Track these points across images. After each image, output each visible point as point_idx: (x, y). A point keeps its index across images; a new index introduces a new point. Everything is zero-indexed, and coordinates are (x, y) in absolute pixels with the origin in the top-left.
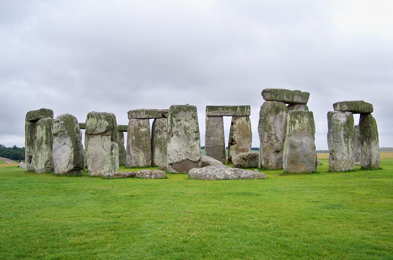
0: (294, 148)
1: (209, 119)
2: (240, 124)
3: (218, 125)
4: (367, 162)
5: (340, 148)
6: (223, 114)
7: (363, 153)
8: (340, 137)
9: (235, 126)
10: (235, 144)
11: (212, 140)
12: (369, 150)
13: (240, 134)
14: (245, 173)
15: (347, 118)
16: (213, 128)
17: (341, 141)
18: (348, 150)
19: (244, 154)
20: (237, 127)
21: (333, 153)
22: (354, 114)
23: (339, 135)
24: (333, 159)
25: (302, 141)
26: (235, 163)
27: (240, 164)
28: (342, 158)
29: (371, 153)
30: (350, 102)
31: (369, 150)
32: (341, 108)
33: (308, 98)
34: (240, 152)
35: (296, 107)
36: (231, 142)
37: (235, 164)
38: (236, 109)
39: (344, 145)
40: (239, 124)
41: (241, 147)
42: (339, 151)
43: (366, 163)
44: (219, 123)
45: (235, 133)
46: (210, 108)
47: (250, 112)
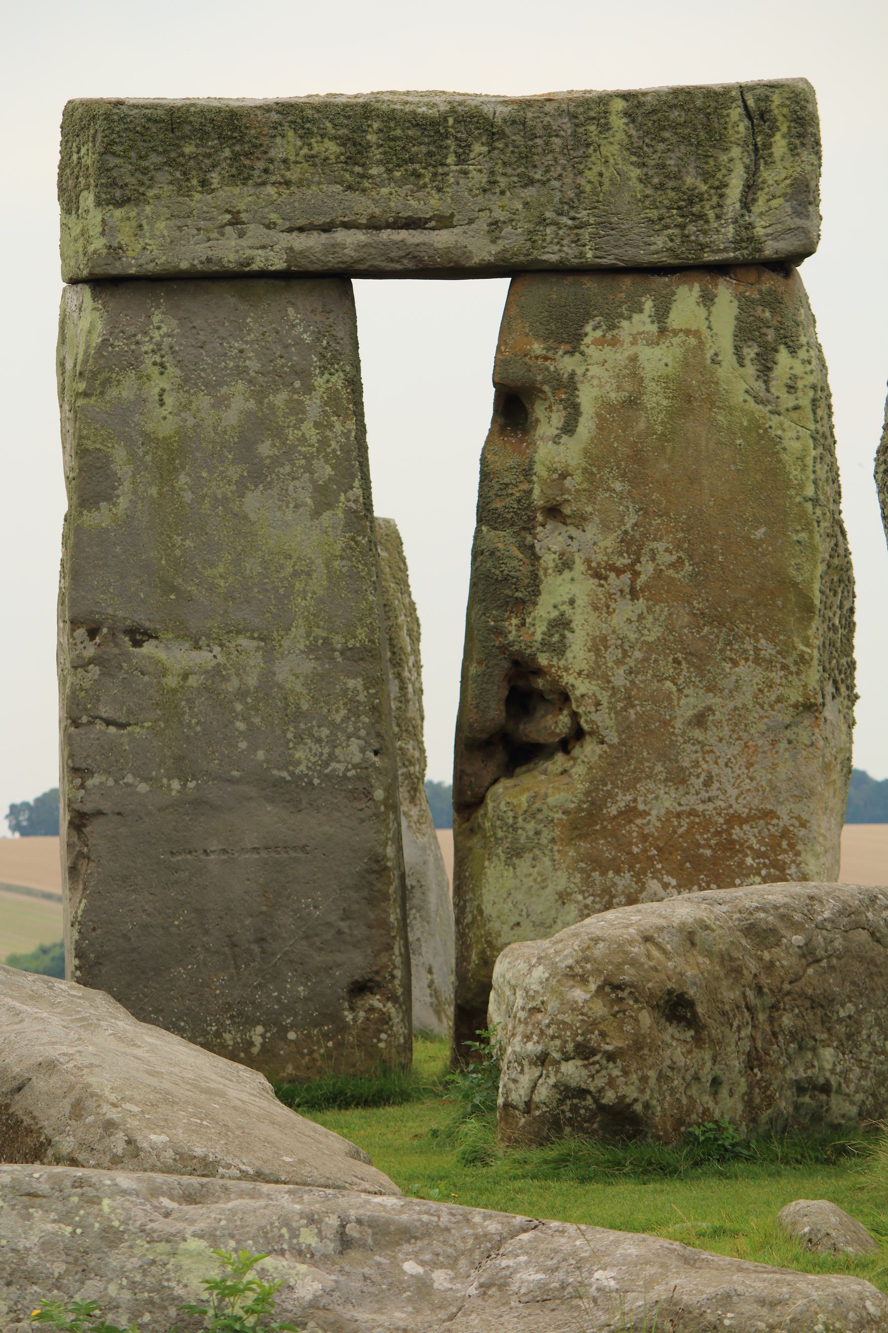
1: (113, 327)
2: (649, 401)
3: (278, 433)
6: (340, 235)
9: (554, 449)
10: (565, 746)
11: (171, 681)
13: (646, 569)
14: (531, 1277)
16: (183, 479)
19: (682, 908)
20: (597, 459)
26: (525, 1080)
27: (609, 1097)
34: (653, 885)
36: (496, 713)
37: (518, 1095)
38: (580, 146)
40: (633, 403)
41: (660, 802)
44: (280, 399)
45: (565, 564)
47: (804, 195)
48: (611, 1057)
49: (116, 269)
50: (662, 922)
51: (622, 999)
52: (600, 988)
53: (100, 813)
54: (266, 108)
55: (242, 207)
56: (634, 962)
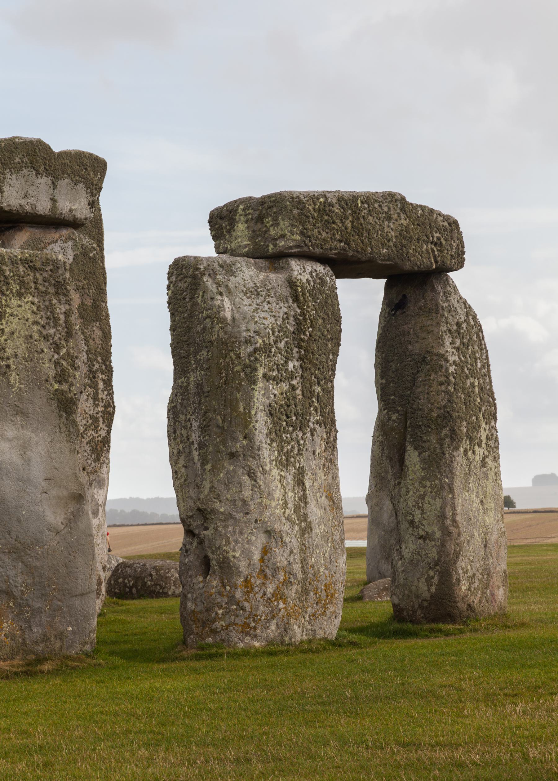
4: (429, 580)
5: (247, 494)
7: (404, 525)
8: (246, 421)
12: (438, 503)
15: (296, 299)
17: (252, 451)
18: (297, 508)
21: (206, 529)
22: (341, 283)
24: (206, 566)
28: (262, 560)
30: (313, 198)
31: (438, 503)
33: (94, 188)
42: (239, 516)
43: (424, 589)
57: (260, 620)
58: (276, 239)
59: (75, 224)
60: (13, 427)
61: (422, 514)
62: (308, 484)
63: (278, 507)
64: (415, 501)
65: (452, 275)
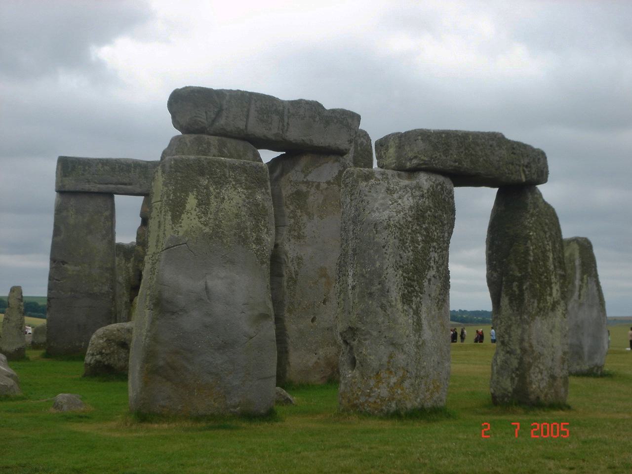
0: (173, 313)
4: (512, 379)
17: (385, 292)
21: (354, 340)
23: (378, 264)
25: (210, 284)
27: (106, 363)
28: (389, 362)
29: (526, 345)
31: (520, 331)
32: (398, 158)
35: (304, 161)
39: (400, 306)
42: (375, 333)
43: (508, 385)
46: (67, 166)
48: (107, 355)
49: (63, 190)
50: (123, 327)
51: (110, 343)
52: (106, 341)
53: (53, 298)
54: (96, 159)
55: (89, 179)
56: (114, 335)
57: (385, 400)
58: (412, 159)
59: (339, 153)
60: (224, 270)
61: (509, 337)
62: (423, 316)
63: (401, 329)
64: (505, 329)
65: (540, 187)
